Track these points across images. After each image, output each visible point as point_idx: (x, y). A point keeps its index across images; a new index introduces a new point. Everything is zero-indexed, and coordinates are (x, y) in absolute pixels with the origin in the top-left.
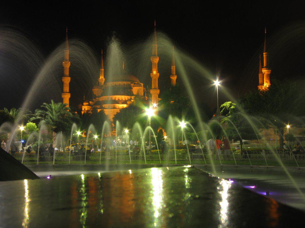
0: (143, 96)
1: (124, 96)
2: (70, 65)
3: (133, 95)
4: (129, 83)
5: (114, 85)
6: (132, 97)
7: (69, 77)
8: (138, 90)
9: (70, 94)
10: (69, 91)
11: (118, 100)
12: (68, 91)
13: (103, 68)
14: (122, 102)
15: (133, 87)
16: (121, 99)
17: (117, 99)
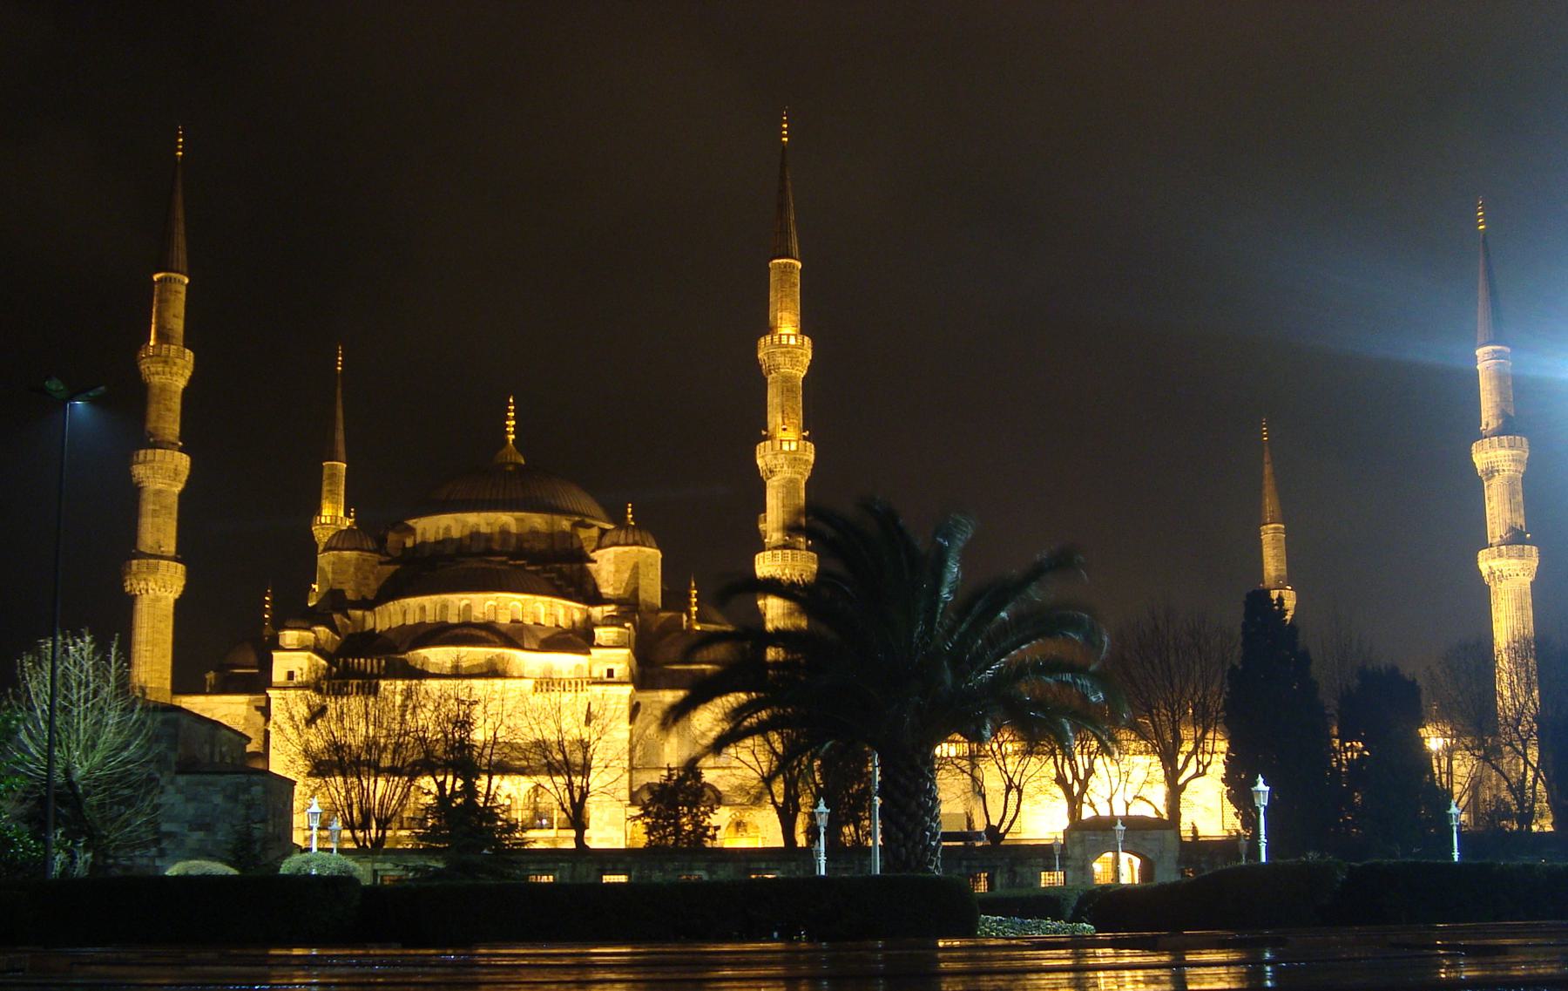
0: (658, 611)
1: (547, 599)
2: (188, 373)
3: (595, 598)
4: (565, 524)
5: (467, 532)
6: (597, 612)
7: (181, 450)
8: (636, 567)
9: (181, 568)
10: (178, 552)
11: (512, 621)
12: (170, 547)
13: (343, 457)
14: (543, 635)
15: (599, 547)
16: (528, 621)
17: (504, 619)
